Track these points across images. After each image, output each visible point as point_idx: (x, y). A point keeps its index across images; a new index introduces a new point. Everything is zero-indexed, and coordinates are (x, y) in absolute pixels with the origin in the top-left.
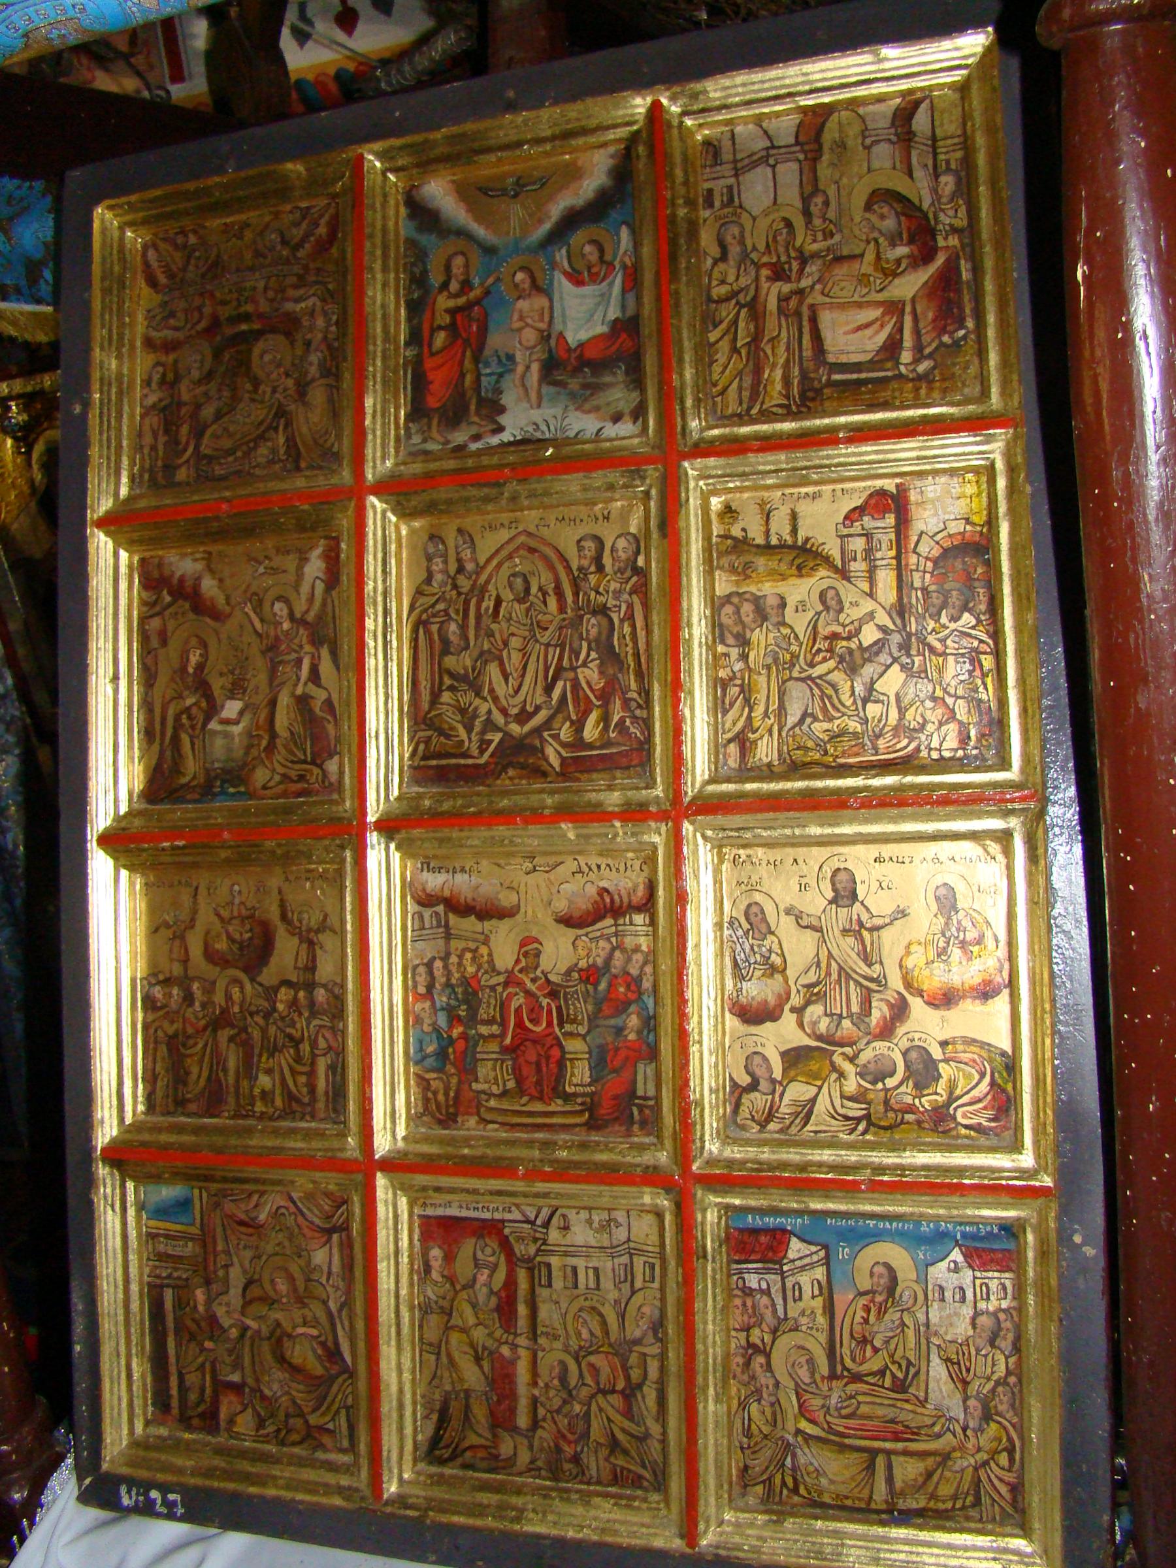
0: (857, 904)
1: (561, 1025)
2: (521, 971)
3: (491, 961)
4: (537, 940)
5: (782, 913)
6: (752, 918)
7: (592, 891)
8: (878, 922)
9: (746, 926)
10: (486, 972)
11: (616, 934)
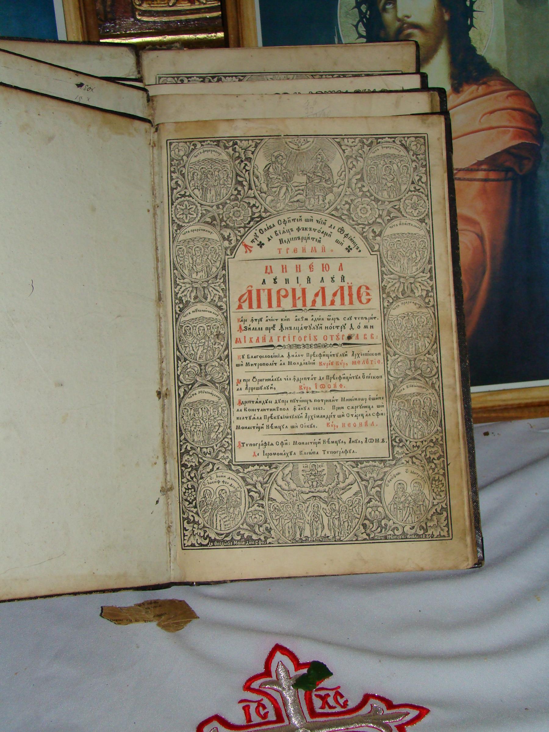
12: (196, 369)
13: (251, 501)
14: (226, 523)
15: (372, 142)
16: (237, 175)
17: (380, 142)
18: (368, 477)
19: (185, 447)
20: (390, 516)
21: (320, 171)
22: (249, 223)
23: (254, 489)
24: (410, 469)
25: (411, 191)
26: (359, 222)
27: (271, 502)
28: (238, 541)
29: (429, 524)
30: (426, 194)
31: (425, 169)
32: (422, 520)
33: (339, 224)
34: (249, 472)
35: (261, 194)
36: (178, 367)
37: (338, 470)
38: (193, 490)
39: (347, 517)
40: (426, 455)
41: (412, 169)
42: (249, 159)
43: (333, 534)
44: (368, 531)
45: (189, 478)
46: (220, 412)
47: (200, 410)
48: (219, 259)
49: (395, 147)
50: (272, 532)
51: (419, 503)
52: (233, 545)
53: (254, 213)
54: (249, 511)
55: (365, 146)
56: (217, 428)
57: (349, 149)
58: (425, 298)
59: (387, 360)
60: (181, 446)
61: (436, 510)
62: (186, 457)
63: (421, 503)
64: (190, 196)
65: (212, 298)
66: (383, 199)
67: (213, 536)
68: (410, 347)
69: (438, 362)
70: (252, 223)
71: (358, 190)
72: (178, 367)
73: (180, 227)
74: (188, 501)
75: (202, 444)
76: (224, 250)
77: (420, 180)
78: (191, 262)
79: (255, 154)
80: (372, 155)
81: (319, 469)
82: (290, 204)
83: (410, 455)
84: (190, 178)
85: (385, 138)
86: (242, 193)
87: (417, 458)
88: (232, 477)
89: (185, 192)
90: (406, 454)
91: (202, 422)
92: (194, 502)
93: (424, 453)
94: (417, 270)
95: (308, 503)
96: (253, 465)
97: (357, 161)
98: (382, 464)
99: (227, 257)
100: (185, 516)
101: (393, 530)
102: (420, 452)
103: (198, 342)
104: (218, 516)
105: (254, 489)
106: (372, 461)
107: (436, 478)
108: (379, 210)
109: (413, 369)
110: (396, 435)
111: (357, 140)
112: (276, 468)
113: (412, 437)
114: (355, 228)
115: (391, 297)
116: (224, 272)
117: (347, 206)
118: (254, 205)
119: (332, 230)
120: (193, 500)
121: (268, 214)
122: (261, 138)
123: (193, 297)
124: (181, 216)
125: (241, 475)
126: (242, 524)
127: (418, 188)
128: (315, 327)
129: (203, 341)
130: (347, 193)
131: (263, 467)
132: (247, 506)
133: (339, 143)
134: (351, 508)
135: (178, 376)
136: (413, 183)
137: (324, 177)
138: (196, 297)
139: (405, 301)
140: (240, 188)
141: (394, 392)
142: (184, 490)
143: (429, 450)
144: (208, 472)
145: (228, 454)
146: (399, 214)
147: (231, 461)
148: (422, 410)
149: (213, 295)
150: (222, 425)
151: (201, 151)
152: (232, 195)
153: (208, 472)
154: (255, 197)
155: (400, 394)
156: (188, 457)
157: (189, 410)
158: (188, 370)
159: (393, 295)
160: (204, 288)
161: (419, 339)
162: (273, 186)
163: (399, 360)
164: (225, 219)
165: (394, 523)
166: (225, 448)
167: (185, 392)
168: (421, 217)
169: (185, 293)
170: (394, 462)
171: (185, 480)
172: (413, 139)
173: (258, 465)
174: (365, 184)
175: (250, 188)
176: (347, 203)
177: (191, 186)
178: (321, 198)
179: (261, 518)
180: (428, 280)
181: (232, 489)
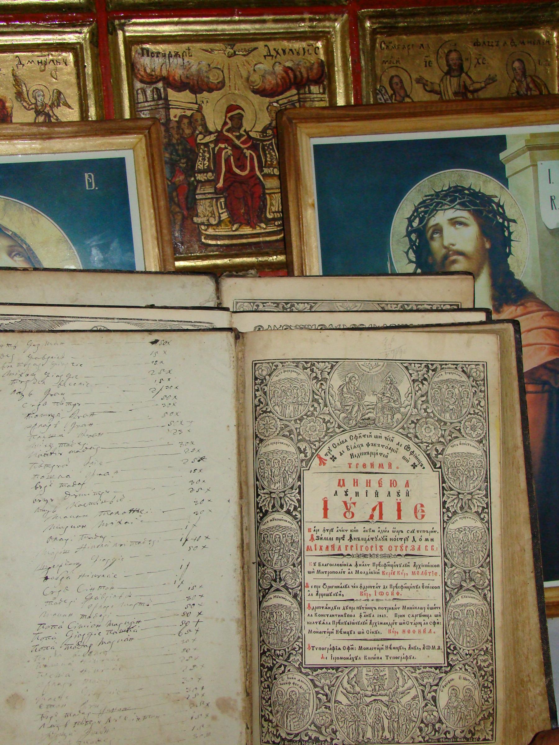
0: (464, 75)
1: (261, 171)
2: (228, 131)
3: (205, 125)
4: (239, 108)
5: (414, 82)
6: (394, 86)
7: (279, 69)
8: (477, 86)
9: (390, 92)
10: (201, 133)
11: (299, 101)
12: (272, 575)
13: (318, 703)
14: (295, 724)
18: (424, 683)
21: (389, 392)
23: (322, 692)
24: (463, 676)
37: (398, 675)
42: (325, 380)
47: (274, 614)
50: (337, 733)
51: (470, 709)
53: (328, 429)
54: (316, 712)
55: (430, 371)
56: (289, 631)
57: (416, 374)
59: (445, 571)
63: (472, 708)
65: (288, 507)
67: (284, 735)
68: (466, 559)
70: (326, 437)
73: (261, 441)
78: (270, 474)
81: (381, 674)
82: (361, 421)
83: (463, 662)
84: (271, 396)
86: (318, 409)
88: (301, 679)
89: (267, 409)
90: (460, 661)
99: (302, 469)
101: (445, 734)
103: (274, 549)
105: (322, 692)
107: (486, 685)
110: (451, 643)
111: (423, 365)
114: (419, 446)
116: (299, 483)
118: (329, 421)
119: (398, 447)
121: (342, 429)
123: (271, 507)
129: (279, 548)
132: (315, 707)
134: (409, 712)
138: (273, 506)
141: (450, 602)
144: (281, 674)
145: (299, 657)
146: (458, 434)
147: (301, 663)
148: (475, 620)
149: (288, 505)
150: (294, 629)
153: (281, 674)
159: (452, 510)
160: (281, 498)
161: (474, 552)
163: (455, 572)
164: (302, 433)
166: (296, 651)
169: (264, 503)
173: (327, 668)
174: (429, 406)
175: (326, 405)
177: (272, 402)
178: (389, 416)
179: (327, 720)
180: (484, 498)
181: (301, 691)
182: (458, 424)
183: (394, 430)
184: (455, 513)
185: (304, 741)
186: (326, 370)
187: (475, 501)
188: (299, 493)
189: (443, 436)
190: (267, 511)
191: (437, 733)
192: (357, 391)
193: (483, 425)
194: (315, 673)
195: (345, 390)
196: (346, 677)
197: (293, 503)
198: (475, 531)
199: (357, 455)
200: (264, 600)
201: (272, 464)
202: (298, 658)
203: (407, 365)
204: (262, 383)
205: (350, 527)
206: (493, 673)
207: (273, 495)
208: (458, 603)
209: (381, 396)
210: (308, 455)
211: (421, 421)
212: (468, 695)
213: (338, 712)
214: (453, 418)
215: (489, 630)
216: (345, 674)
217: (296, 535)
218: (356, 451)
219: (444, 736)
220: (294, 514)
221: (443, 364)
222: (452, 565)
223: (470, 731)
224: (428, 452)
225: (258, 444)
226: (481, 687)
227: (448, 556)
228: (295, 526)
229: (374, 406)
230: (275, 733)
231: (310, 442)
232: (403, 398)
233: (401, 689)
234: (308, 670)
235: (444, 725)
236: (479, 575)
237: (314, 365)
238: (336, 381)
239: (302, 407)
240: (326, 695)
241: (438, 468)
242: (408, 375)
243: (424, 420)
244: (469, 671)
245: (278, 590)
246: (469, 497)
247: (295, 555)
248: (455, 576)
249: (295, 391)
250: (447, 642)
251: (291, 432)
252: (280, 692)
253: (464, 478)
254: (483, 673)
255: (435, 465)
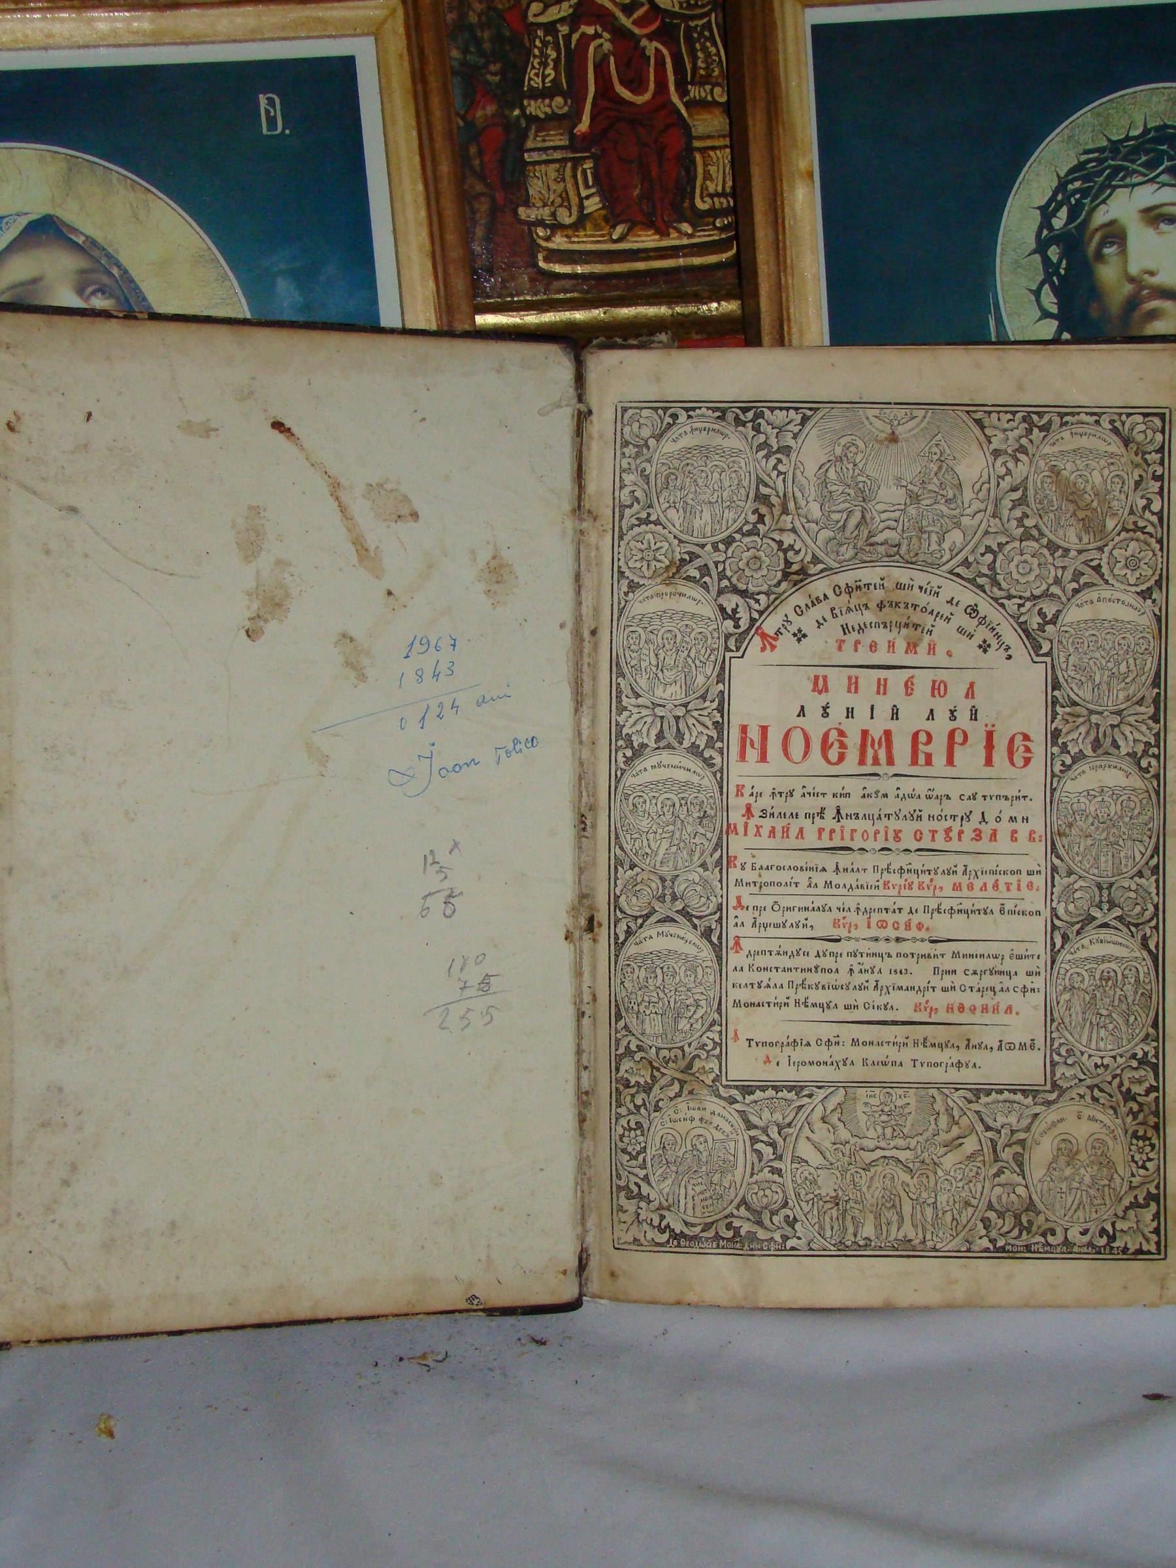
12: (653, 885)
13: (756, 1161)
14: (705, 1203)
15: (1050, 422)
16: (760, 481)
17: (1067, 423)
18: (998, 1125)
19: (625, 1044)
20: (1040, 1206)
21: (935, 480)
22: (779, 583)
23: (765, 1138)
24: (1087, 1112)
25: (1128, 531)
26: (1013, 592)
27: (798, 1166)
28: (728, 1240)
29: (1118, 1226)
30: (1159, 536)
31: (1158, 484)
32: (1105, 1217)
33: (967, 597)
34: (756, 1102)
35: (806, 525)
36: (616, 879)
37: (939, 1106)
38: (638, 1132)
39: (951, 1203)
40: (1121, 1084)
41: (1132, 485)
42: (786, 450)
43: (921, 1236)
44: (993, 1234)
45: (631, 1106)
46: (700, 977)
47: (659, 971)
48: (713, 658)
49: (1098, 434)
50: (798, 1226)
51: (1102, 1183)
52: (718, 1247)
53: (788, 564)
54: (751, 1180)
55: (1036, 430)
56: (692, 1009)
57: (1001, 435)
58: (1142, 756)
59: (1053, 886)
60: (618, 1041)
61: (1136, 1197)
62: (626, 1065)
63: (1107, 1182)
64: (657, 523)
65: (693, 740)
66: (1065, 545)
67: (678, 1227)
68: (1103, 859)
69: (1158, 894)
70: (784, 585)
71: (1015, 523)
72: (616, 879)
73: (633, 587)
74: (629, 1154)
75: (660, 1040)
76: (722, 639)
77: (1146, 507)
78: (654, 662)
79: (800, 441)
80: (1047, 449)
81: (900, 1103)
82: (867, 548)
83: (1089, 1082)
84: (659, 484)
85: (1078, 414)
86: (767, 519)
87: (1101, 1090)
88: (718, 1110)
89: (649, 515)
90: (1081, 1080)
91: (661, 995)
92: (641, 1158)
93: (1117, 1080)
94: (1128, 699)
95: (873, 1170)
96: (763, 1089)
97: (1017, 460)
98: (1030, 1098)
99: (728, 655)
100: (622, 1183)
101: (1044, 1235)
102: (1109, 1078)
103: (660, 831)
104: (690, 1187)
105: (765, 1138)
106: (1009, 1091)
107: (1141, 1133)
108: (1056, 568)
109: (1105, 906)
110: (1062, 1041)
111: (1019, 416)
112: (810, 1096)
113: (1093, 1046)
114: (1002, 605)
115: (1068, 752)
116: (720, 687)
117: (989, 557)
118: (791, 547)
119: (953, 609)
120: (638, 1153)
121: (820, 567)
122: (815, 406)
123: (653, 738)
124: (638, 565)
125: (737, 1106)
126: (738, 1208)
127: (1141, 524)
128: (908, 816)
129: (671, 828)
130: (990, 530)
131: (784, 1094)
132: (749, 1170)
133: (979, 422)
134: (960, 1184)
135: (617, 898)
136: (1132, 512)
137: (944, 493)
138: (660, 736)
139: (1098, 763)
140: (763, 510)
141: (1064, 952)
142: (620, 1131)
143: (1127, 1075)
144: (671, 1099)
145: (713, 1064)
146: (1096, 579)
147: (717, 1079)
148: (1119, 992)
149: (695, 734)
150: (703, 1003)
151: (688, 429)
152: (747, 522)
153: (671, 1099)
154: (794, 530)
155: (1075, 956)
156: (631, 1064)
157: (636, 969)
158: (638, 888)
159: (1073, 750)
160: (677, 718)
161: (1121, 843)
162: (834, 508)
163: (1076, 886)
164: (729, 573)
165: (1047, 1220)
166: (708, 1052)
167: (629, 933)
168: (1144, 587)
169: (638, 727)
170: (1054, 1096)
171: (623, 1111)
172: (1140, 419)
173: (774, 1087)
174: (1029, 512)
175: (785, 511)
176: (989, 549)
177: (661, 500)
178: (934, 537)
179: (776, 1197)
180: (1150, 722)
181: (718, 1135)
182: (1095, 554)
183: (944, 568)
184: (1079, 757)
185: (723, 1239)
186: (790, 427)
187: (1127, 730)
188: (720, 710)
189: (1057, 581)
190: (644, 746)
191: (1025, 1233)
192: (860, 479)
193: (1154, 555)
194: (749, 1099)
195: (832, 474)
196: (820, 1108)
197: (705, 731)
198: (1125, 797)
199: (857, 627)
200: (632, 939)
201: (660, 641)
202: (711, 1065)
203: (978, 415)
204: (638, 455)
205: (836, 785)
206: (1157, 1105)
207: (660, 712)
208: (1083, 954)
209: (916, 489)
210: (741, 623)
211: (1009, 547)
212: (1099, 1153)
213: (799, 1182)
214: (1085, 540)
215: (1152, 1014)
216: (816, 1102)
217: (711, 801)
218: (853, 619)
219: (1043, 1240)
220: (707, 754)
221: (1066, 414)
222: (1070, 873)
223: (1103, 1232)
224: (1022, 619)
225: (626, 594)
226: (1129, 1136)
227: (1061, 851)
228: (708, 782)
229: (897, 514)
230: (656, 1223)
231: (744, 594)
232: (968, 494)
233: (944, 1137)
234: (734, 1092)
235: (1041, 1218)
236: (1133, 895)
237: (762, 415)
238: (811, 451)
239: (731, 514)
240: (773, 1145)
241: (1043, 655)
242: (982, 438)
243: (1017, 544)
244: (1102, 1101)
245: (668, 920)
246: (1115, 720)
247: (706, 843)
248: (1078, 895)
249: (716, 475)
250: (1052, 1040)
251: (705, 570)
252: (670, 1137)
253: (1105, 678)
254: (1136, 1108)
255: (1037, 647)
